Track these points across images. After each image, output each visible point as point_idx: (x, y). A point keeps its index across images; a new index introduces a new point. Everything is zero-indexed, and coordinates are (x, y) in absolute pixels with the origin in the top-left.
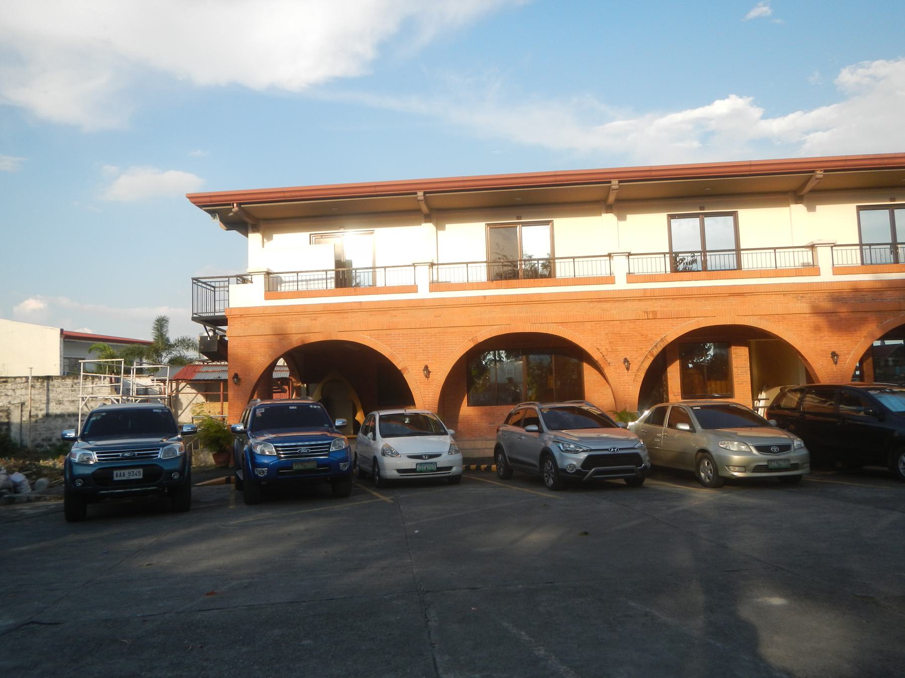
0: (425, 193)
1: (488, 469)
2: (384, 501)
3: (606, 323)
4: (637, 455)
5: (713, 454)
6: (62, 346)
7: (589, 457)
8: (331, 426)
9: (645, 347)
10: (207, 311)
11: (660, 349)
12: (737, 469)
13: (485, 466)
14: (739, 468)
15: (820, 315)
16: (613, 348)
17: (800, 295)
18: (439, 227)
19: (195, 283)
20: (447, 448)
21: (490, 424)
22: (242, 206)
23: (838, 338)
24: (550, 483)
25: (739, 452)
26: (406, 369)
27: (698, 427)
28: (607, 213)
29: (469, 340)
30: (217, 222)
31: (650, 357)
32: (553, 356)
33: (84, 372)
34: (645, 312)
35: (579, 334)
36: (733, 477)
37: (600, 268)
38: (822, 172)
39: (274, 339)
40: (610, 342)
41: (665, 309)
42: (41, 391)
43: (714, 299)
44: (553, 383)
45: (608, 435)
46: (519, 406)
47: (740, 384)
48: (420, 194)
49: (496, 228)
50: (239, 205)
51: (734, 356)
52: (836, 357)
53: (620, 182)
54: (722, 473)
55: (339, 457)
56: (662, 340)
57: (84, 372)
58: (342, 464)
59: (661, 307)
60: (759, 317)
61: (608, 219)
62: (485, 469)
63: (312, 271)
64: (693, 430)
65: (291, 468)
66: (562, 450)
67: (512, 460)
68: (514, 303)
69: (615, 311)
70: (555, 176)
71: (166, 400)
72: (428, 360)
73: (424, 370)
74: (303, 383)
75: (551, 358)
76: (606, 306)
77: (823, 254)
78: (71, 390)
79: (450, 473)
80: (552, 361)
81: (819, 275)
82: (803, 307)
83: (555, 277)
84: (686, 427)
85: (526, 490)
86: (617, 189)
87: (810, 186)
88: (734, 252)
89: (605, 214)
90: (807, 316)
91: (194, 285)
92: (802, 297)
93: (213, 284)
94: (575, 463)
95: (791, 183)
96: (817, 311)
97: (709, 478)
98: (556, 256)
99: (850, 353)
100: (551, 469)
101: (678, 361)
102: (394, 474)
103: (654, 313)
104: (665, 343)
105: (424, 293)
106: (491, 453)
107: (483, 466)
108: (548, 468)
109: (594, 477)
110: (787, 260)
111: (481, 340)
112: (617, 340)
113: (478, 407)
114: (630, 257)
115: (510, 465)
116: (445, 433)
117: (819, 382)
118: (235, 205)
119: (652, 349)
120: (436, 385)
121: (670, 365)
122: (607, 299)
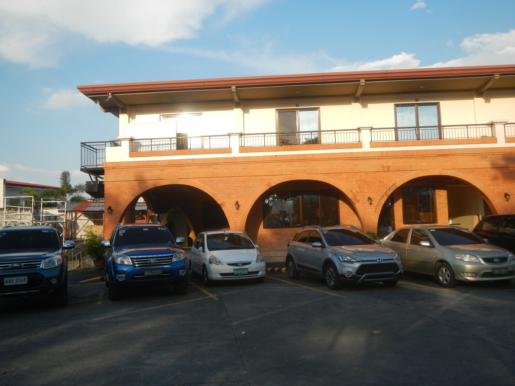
0: (237, 87)
1: (280, 271)
2: (212, 299)
3: (356, 174)
4: (395, 264)
5: (451, 264)
6: (5, 190)
7: (361, 267)
8: (173, 243)
9: (382, 190)
10: (92, 165)
11: (392, 191)
12: (469, 274)
13: (277, 269)
14: (473, 274)
16: (361, 190)
17: (484, 156)
18: (245, 111)
20: (255, 258)
21: (278, 240)
22: (115, 95)
23: (508, 184)
24: (331, 284)
25: (469, 263)
26: (223, 204)
27: (436, 244)
28: (355, 102)
29: (266, 185)
30: (98, 106)
31: (385, 196)
32: (319, 196)
33: (6, 205)
34: (382, 167)
35: (338, 181)
36: (467, 281)
37: (353, 138)
38: (498, 75)
39: (135, 183)
40: (359, 187)
41: (395, 165)
43: (427, 158)
44: (319, 213)
45: (363, 249)
46: (304, 229)
47: (441, 214)
48: (234, 88)
49: (282, 112)
50: (113, 94)
51: (437, 196)
52: (508, 197)
53: (366, 81)
54: (458, 278)
55: (179, 265)
56: (393, 185)
57: (6, 205)
58: (181, 271)
59: (393, 163)
61: (356, 106)
62: (278, 271)
63: (161, 139)
64: (432, 246)
65: (143, 274)
66: (341, 261)
67: (299, 266)
68: (296, 161)
69: (363, 166)
70: (323, 76)
71: (64, 223)
72: (239, 198)
73: (235, 205)
74: (155, 213)
75: (318, 197)
77: (499, 129)
78: (7, 217)
79: (257, 275)
80: (318, 199)
82: (486, 164)
83: (321, 143)
84: (427, 244)
85: (315, 289)
86: (363, 86)
87: (489, 86)
88: (437, 128)
89: (354, 103)
90: (488, 169)
91: (82, 147)
93: (95, 147)
94: (351, 270)
95: (475, 83)
96: (495, 167)
97: (446, 281)
98: (322, 130)
100: (333, 274)
101: (401, 201)
102: (219, 277)
103: (388, 167)
104: (396, 187)
105: (236, 153)
106: (284, 260)
107: (276, 269)
108: (330, 273)
109: (365, 280)
110: (474, 133)
112: (364, 185)
113: (270, 229)
114: (372, 130)
115: (298, 269)
116: (253, 248)
117: (496, 213)
118: (110, 94)
119: (386, 191)
120: (243, 214)
122: (357, 158)
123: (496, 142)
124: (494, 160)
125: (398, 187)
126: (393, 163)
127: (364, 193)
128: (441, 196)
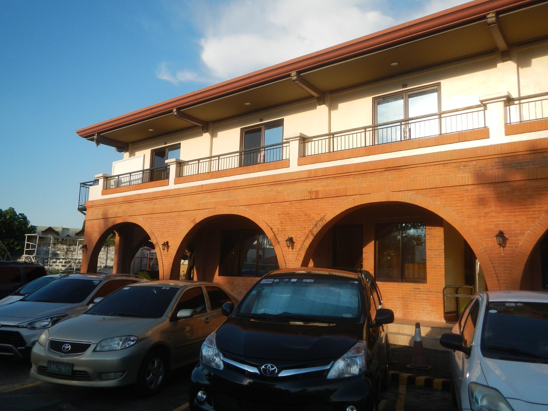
3: (279, 205)
9: (307, 226)
11: (319, 228)
15: (487, 185)
16: (283, 227)
17: (463, 163)
19: (82, 186)
23: (507, 214)
29: (191, 221)
31: (310, 236)
33: (27, 241)
34: (309, 192)
39: (102, 221)
40: (281, 222)
41: (327, 188)
42: (104, 253)
56: (321, 219)
60: (415, 192)
72: (169, 237)
76: (280, 188)
81: (489, 138)
90: (470, 188)
92: (465, 166)
99: (523, 234)
103: (317, 192)
104: (325, 223)
111: (198, 221)
112: (287, 220)
119: (312, 229)
120: (171, 257)
121: (365, 246)
122: (282, 182)
123: (488, 137)
124: (482, 170)
125: (327, 222)
126: (323, 186)
127: (286, 232)
128: (434, 237)
